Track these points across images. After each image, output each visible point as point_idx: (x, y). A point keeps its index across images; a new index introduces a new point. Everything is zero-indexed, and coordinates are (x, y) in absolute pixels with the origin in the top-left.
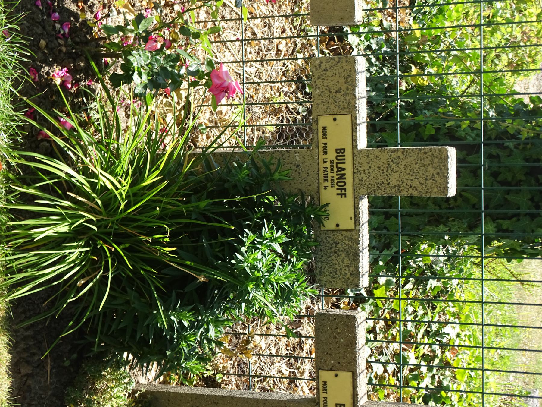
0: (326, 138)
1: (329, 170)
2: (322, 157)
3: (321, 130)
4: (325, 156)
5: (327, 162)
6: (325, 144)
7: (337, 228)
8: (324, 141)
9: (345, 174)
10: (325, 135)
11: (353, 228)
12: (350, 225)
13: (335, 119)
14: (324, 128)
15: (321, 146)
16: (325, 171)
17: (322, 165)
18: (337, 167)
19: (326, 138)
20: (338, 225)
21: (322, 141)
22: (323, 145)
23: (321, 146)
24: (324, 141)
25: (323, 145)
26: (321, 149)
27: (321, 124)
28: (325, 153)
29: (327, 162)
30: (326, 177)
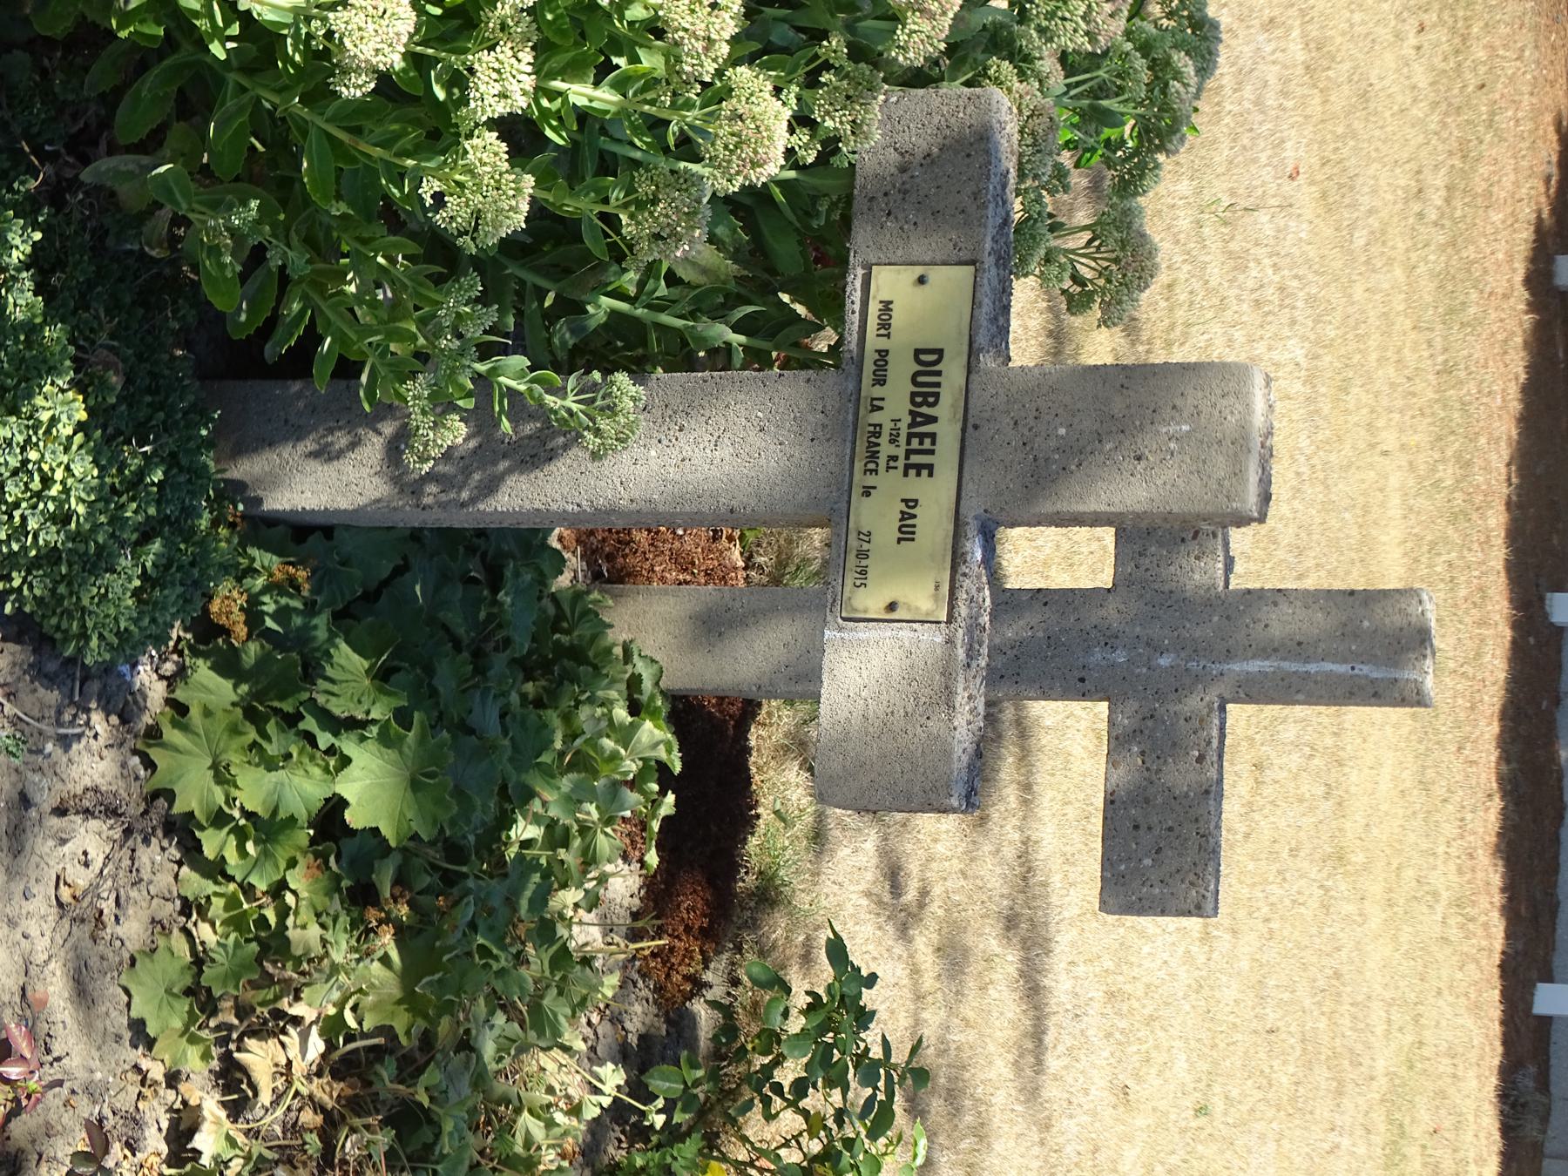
0: (888, 336)
2: (869, 389)
3: (874, 308)
4: (878, 391)
6: (883, 354)
10: (885, 325)
13: (921, 280)
14: (887, 306)
19: (888, 336)
22: (877, 356)
24: (883, 343)
25: (877, 356)
26: (869, 367)
28: (880, 381)
30: (873, 456)
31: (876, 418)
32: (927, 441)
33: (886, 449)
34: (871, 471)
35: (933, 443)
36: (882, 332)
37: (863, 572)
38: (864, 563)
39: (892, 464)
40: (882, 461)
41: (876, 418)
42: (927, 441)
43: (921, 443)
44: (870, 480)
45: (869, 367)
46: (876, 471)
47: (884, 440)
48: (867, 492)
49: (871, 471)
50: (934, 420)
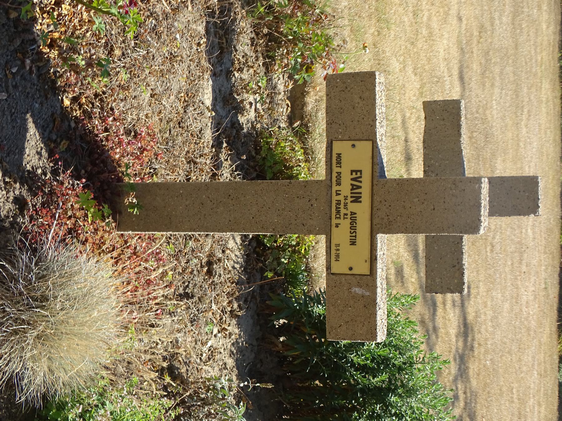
0: (340, 167)
2: (335, 188)
4: (338, 188)
5: (340, 194)
6: (339, 174)
7: (350, 272)
8: (338, 170)
9: (361, 197)
10: (339, 163)
12: (364, 269)
14: (339, 155)
16: (337, 204)
17: (335, 198)
19: (340, 167)
20: (351, 269)
21: (335, 169)
22: (337, 175)
23: (334, 175)
24: (338, 170)
25: (337, 175)
26: (334, 179)
27: (335, 151)
28: (339, 184)
29: (340, 194)
30: (338, 212)
31: (338, 198)
33: (343, 211)
34: (338, 218)
36: (338, 165)
37: (338, 256)
38: (338, 252)
40: (342, 214)
41: (338, 198)
44: (338, 221)
45: (334, 179)
46: (340, 218)
47: (342, 206)
48: (337, 226)
49: (338, 218)
50: (360, 187)
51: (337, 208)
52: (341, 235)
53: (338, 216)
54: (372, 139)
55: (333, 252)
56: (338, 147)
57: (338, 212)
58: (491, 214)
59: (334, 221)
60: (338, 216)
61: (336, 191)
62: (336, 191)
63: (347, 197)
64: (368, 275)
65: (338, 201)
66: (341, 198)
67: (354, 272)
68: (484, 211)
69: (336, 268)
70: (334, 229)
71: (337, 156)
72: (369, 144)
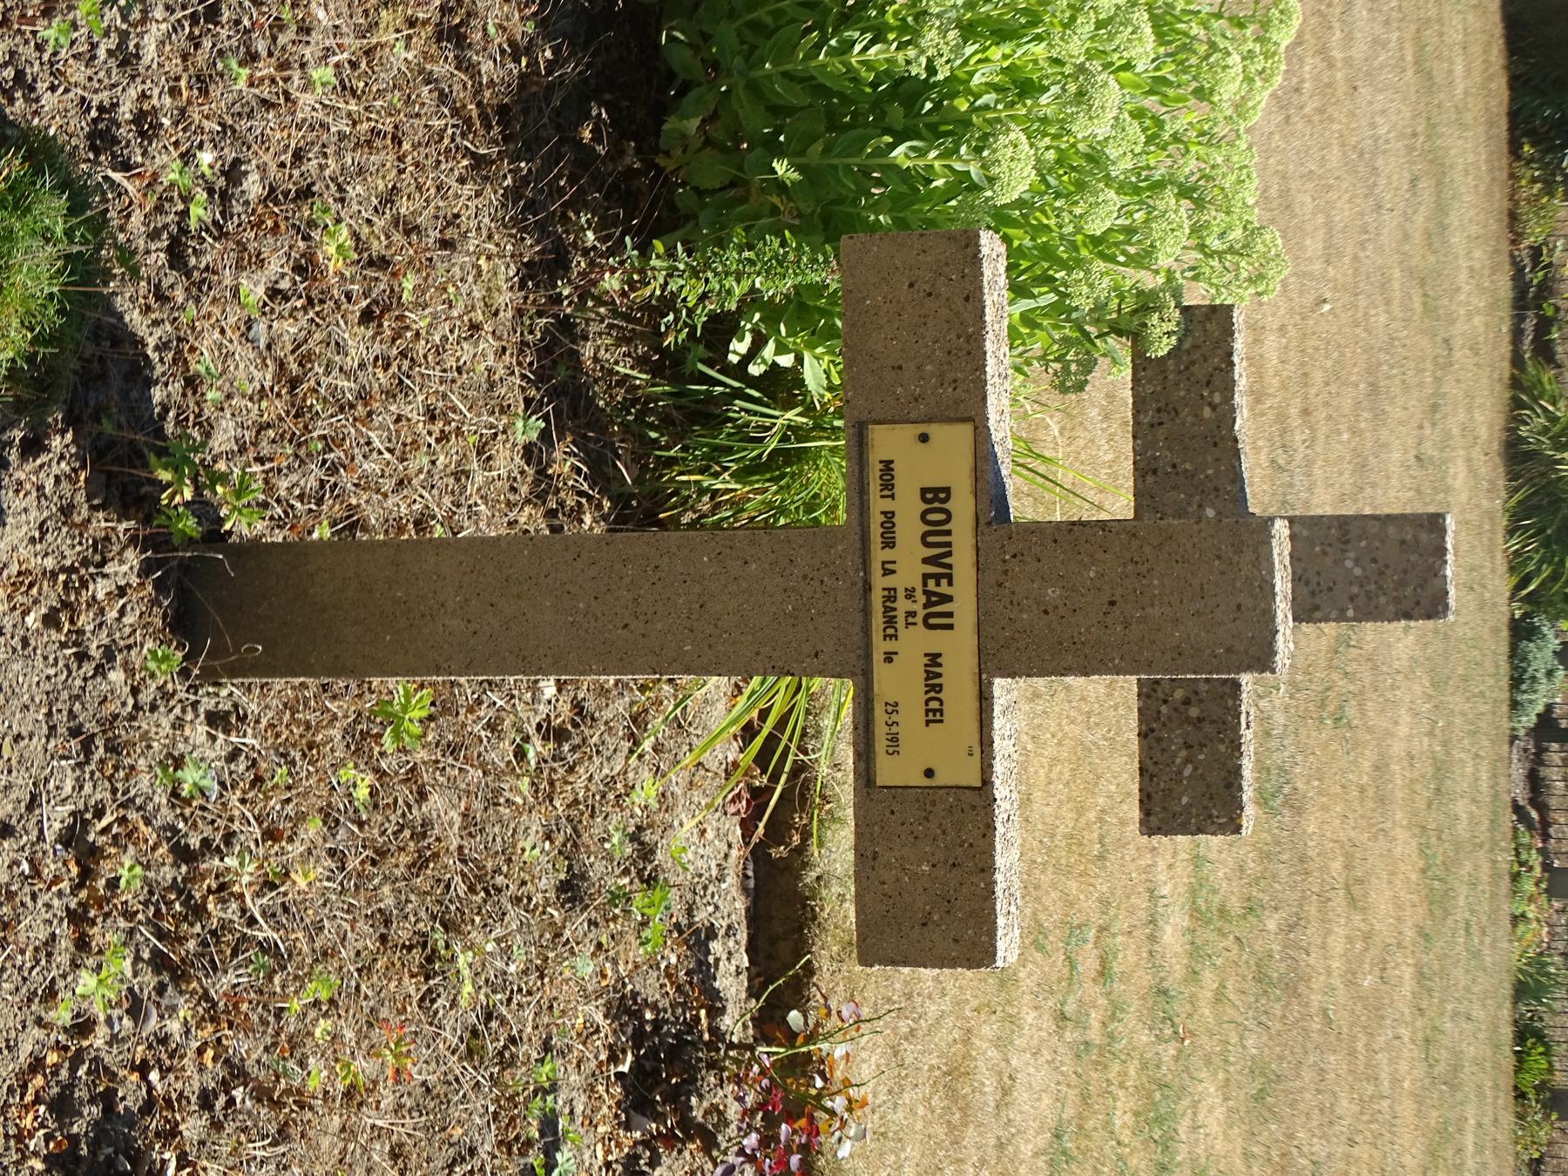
0: (892, 497)
1: (901, 594)
2: (879, 555)
4: (888, 554)
5: (893, 572)
6: (889, 515)
7: (926, 782)
8: (887, 505)
10: (888, 486)
11: (979, 784)
14: (887, 466)
15: (876, 520)
17: (879, 582)
18: (925, 592)
19: (892, 497)
20: (929, 773)
21: (878, 505)
22: (883, 518)
23: (876, 520)
24: (887, 505)
25: (883, 518)
28: (889, 543)
29: (893, 572)
30: (890, 621)
31: (890, 581)
32: (944, 582)
34: (891, 636)
35: (950, 584)
36: (886, 492)
37: (894, 739)
38: (894, 729)
39: (911, 620)
41: (890, 581)
42: (944, 582)
43: (938, 584)
44: (890, 646)
48: (889, 658)
49: (891, 636)
51: (887, 610)
52: (898, 681)
53: (890, 631)
54: (976, 418)
55: (881, 731)
56: (887, 441)
57: (890, 621)
58: (1304, 613)
59: (880, 646)
60: (890, 631)
61: (884, 563)
62: (884, 563)
63: (914, 590)
64: (975, 789)
65: (889, 590)
66: (898, 582)
67: (939, 780)
68: (1283, 609)
69: (889, 772)
70: (880, 669)
71: (881, 466)
72: (966, 430)
